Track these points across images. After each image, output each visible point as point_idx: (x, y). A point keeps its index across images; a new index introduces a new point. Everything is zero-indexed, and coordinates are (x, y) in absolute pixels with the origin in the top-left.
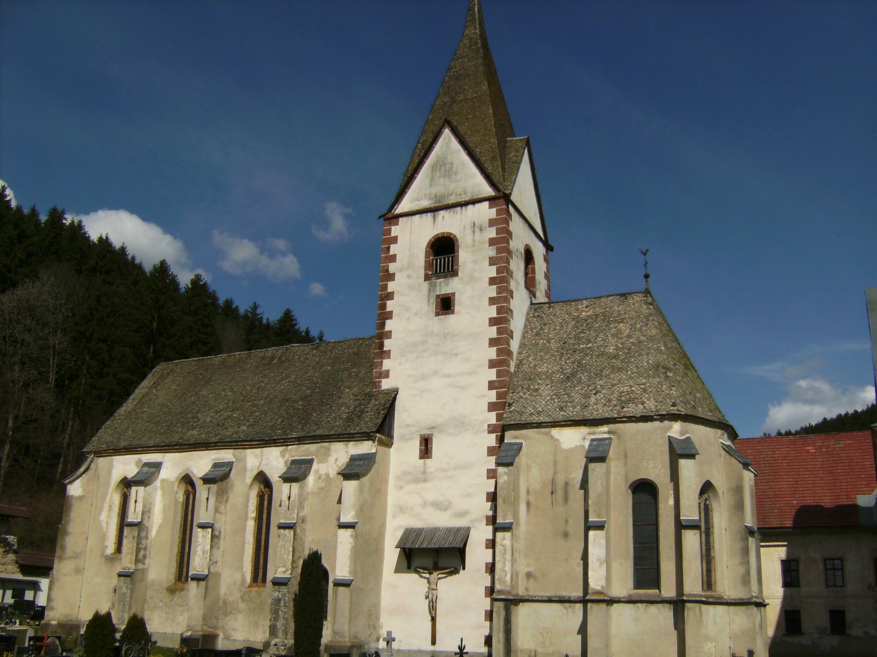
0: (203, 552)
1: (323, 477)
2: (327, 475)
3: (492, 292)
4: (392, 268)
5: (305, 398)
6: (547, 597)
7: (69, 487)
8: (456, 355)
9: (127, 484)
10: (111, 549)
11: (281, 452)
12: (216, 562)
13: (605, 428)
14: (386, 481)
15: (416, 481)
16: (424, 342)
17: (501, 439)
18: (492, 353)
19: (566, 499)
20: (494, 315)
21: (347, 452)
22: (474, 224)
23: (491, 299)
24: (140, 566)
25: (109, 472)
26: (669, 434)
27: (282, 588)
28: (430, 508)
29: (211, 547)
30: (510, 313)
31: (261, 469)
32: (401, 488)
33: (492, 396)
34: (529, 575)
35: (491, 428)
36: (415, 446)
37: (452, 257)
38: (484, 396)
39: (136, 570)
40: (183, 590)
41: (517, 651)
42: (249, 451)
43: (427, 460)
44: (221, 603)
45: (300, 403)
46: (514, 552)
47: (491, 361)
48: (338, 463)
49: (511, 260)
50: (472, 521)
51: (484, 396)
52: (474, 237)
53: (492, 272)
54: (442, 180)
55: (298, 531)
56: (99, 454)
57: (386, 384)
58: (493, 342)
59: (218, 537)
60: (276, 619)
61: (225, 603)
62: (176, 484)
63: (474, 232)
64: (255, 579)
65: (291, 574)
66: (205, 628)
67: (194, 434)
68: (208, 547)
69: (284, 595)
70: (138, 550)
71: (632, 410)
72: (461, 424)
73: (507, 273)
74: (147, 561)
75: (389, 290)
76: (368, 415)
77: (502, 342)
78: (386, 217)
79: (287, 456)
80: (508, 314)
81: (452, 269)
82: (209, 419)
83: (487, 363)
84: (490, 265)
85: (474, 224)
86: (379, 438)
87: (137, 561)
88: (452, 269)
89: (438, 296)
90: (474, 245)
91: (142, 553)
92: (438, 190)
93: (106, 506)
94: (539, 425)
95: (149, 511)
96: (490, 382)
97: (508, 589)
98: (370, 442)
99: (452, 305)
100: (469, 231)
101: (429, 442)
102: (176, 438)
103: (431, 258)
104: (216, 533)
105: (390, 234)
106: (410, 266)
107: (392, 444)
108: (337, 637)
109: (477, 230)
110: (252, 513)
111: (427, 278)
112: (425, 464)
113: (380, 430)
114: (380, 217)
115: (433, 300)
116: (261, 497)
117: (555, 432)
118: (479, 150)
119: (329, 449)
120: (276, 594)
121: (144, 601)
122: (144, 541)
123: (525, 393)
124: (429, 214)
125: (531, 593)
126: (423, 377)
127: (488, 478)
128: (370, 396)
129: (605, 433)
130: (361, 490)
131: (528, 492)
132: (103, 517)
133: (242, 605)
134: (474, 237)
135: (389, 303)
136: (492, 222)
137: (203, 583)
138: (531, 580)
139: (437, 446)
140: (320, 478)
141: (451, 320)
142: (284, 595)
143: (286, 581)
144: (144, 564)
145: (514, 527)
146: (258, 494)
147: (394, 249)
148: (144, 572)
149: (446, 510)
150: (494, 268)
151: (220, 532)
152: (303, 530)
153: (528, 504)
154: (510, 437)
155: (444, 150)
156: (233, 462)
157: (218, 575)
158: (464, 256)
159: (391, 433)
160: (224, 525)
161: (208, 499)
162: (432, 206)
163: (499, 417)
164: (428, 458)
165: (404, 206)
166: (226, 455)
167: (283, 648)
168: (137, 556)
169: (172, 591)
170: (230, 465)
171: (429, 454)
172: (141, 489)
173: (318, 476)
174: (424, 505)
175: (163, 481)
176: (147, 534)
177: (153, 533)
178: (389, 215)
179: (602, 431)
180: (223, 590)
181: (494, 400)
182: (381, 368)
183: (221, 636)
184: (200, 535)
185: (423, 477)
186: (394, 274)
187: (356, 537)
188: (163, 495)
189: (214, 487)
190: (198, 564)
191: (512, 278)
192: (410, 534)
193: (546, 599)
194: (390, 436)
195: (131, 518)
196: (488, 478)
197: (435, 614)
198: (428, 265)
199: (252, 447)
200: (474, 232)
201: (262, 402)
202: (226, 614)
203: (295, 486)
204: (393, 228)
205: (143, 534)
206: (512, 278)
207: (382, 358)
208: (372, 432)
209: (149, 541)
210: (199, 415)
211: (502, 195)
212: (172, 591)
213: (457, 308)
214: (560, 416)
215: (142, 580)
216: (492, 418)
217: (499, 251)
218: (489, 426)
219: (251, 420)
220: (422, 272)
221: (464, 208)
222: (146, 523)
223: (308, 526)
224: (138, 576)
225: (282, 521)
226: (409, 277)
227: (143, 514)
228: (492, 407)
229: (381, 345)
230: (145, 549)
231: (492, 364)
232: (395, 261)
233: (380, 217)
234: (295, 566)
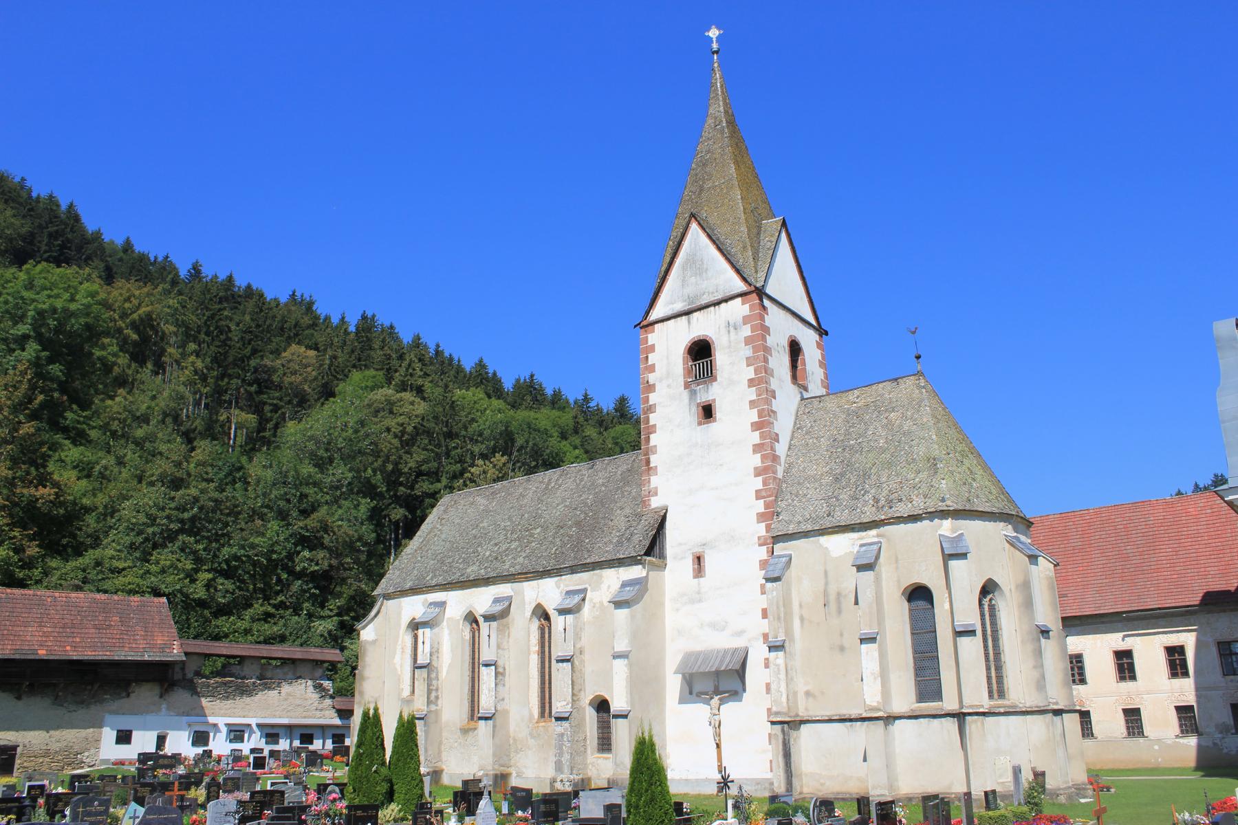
1: (597, 605)
2: (601, 603)
3: (752, 394)
4: (652, 378)
5: (578, 524)
6: (828, 716)
7: (362, 632)
8: (721, 465)
9: (415, 626)
10: (406, 692)
11: (556, 583)
12: (503, 699)
13: (874, 532)
14: (663, 604)
15: (692, 601)
18: (757, 460)
19: (839, 611)
20: (756, 419)
21: (618, 578)
22: (729, 323)
24: (433, 707)
25: (399, 614)
27: (564, 722)
29: (496, 685)
30: (772, 414)
31: (538, 601)
32: (677, 610)
33: (760, 506)
34: (808, 694)
35: (762, 541)
36: (689, 565)
37: (711, 361)
39: (430, 712)
40: (475, 729)
41: (801, 775)
42: (526, 584)
43: (701, 579)
44: (511, 742)
45: (574, 529)
46: (790, 672)
47: (756, 469)
48: (610, 590)
49: (769, 357)
50: (749, 641)
52: (729, 337)
53: (750, 373)
54: (693, 280)
55: (576, 662)
56: (387, 597)
57: (655, 503)
58: (757, 448)
59: (503, 674)
60: (561, 754)
61: (515, 740)
62: (461, 622)
63: (729, 332)
64: (542, 714)
65: (572, 707)
66: (496, 767)
67: (472, 571)
68: (493, 685)
69: (566, 730)
70: (429, 692)
71: (903, 509)
73: (766, 372)
74: (439, 702)
75: (651, 403)
76: (636, 539)
78: (641, 325)
79: (562, 585)
80: (770, 416)
81: (711, 373)
82: (488, 553)
83: (752, 471)
84: (748, 365)
85: (729, 323)
86: (649, 561)
87: (429, 702)
88: (711, 373)
89: (698, 405)
90: (729, 347)
91: (433, 695)
92: (690, 290)
93: (399, 647)
94: (806, 534)
95: (438, 651)
97: (785, 710)
98: (640, 567)
99: (713, 412)
100: (723, 331)
101: (702, 560)
102: (454, 578)
103: (690, 364)
104: (500, 670)
105: (647, 343)
107: (666, 565)
108: (618, 769)
109: (732, 329)
110: (535, 648)
111: (687, 386)
112: (699, 584)
113: (648, 553)
114: (635, 326)
115: (694, 409)
116: (542, 629)
117: (824, 540)
118: (729, 242)
119: (601, 576)
121: (440, 743)
122: (434, 682)
123: (793, 500)
124: (684, 317)
125: (811, 713)
128: (639, 516)
129: (873, 536)
130: (633, 617)
131: (801, 606)
132: (397, 659)
133: (531, 742)
134: (729, 337)
135: (651, 416)
136: (746, 320)
137: (490, 722)
138: (811, 699)
140: (594, 607)
141: (713, 427)
142: (566, 730)
143: (567, 715)
144: (437, 705)
145: (787, 645)
146: (539, 627)
147: (652, 358)
148: (437, 713)
149: (723, 630)
150: (752, 369)
151: (504, 669)
152: (582, 662)
153: (802, 619)
154: (780, 549)
155: (693, 246)
156: (512, 597)
157: (506, 712)
158: (721, 358)
159: (663, 553)
160: (509, 661)
161: (489, 636)
162: (686, 308)
163: (768, 528)
164: (701, 577)
166: (504, 589)
167: (568, 783)
168: (428, 698)
169: (465, 731)
170: (510, 599)
171: (703, 573)
172: (427, 631)
173: (592, 605)
175: (449, 619)
176: (437, 675)
177: (443, 673)
178: (645, 323)
179: (871, 535)
180: (512, 727)
181: (762, 510)
183: (514, 774)
184: (485, 673)
185: (697, 598)
186: (654, 385)
187: (630, 666)
188: (449, 634)
189: (494, 624)
190: (486, 702)
191: (773, 377)
192: (689, 658)
193: (827, 718)
194: (662, 556)
195: (421, 660)
197: (719, 740)
198: (688, 372)
199: (528, 580)
200: (729, 332)
201: (538, 530)
202: (517, 752)
203: (570, 618)
204: (650, 336)
205: (433, 675)
206: (773, 377)
207: (649, 475)
208: (639, 555)
210: (479, 549)
211: (753, 289)
212: (465, 731)
214: (828, 523)
215: (436, 722)
217: (755, 350)
218: (759, 538)
219: (528, 551)
220: (681, 381)
221: (717, 307)
222: (434, 663)
223: (586, 657)
224: (432, 718)
225: (560, 654)
226: (669, 386)
227: (431, 655)
229: (648, 462)
230: (437, 690)
231: (758, 472)
232: (654, 371)
233: (635, 326)
234: (575, 699)
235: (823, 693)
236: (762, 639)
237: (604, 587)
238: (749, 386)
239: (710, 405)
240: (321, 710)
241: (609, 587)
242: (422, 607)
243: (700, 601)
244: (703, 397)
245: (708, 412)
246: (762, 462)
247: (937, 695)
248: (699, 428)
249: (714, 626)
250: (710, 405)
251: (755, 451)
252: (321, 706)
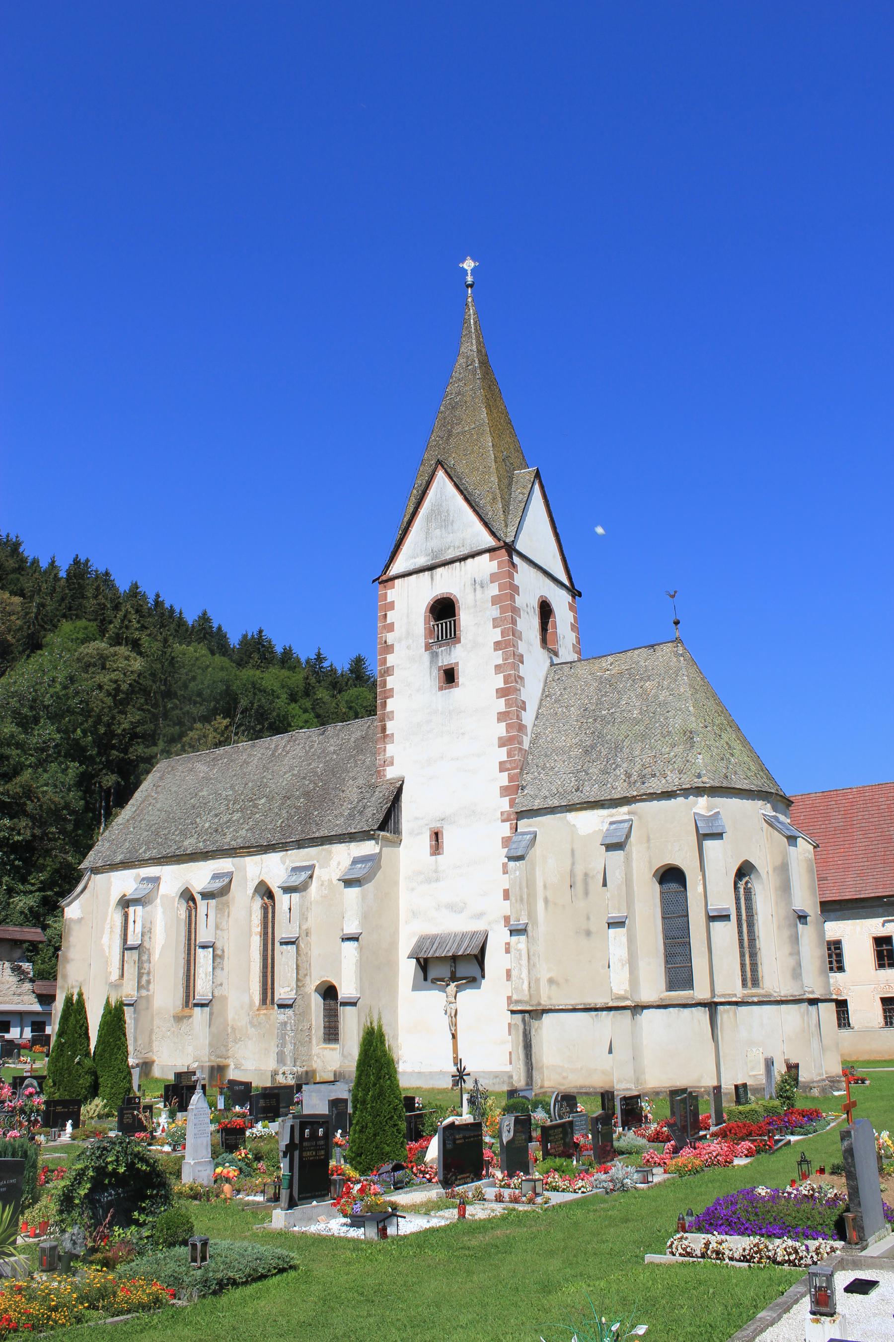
1: (326, 883)
2: (330, 881)
3: (498, 658)
4: (390, 638)
5: (306, 794)
6: (572, 1005)
7: (66, 909)
8: (463, 734)
9: (125, 903)
10: (115, 976)
12: (221, 985)
13: (625, 809)
14: (396, 883)
15: (429, 881)
18: (501, 730)
19: (586, 893)
20: (502, 685)
21: (349, 854)
22: (475, 581)
24: (144, 993)
25: (109, 890)
27: (287, 1010)
30: (519, 680)
31: (262, 878)
32: (413, 889)
33: (504, 779)
34: (551, 981)
36: (426, 841)
37: (455, 621)
39: (140, 997)
40: (190, 1016)
41: (542, 1068)
42: (248, 859)
44: (230, 1030)
45: (302, 800)
46: (532, 957)
47: (500, 739)
48: (340, 867)
49: (518, 619)
50: (489, 923)
52: (475, 596)
53: (496, 635)
54: (438, 532)
55: (302, 945)
56: (96, 871)
57: (391, 773)
58: (502, 717)
59: (222, 957)
60: (283, 1045)
61: (233, 1029)
62: (177, 899)
63: (475, 590)
64: (264, 1001)
65: (296, 994)
66: (213, 1058)
67: (190, 844)
68: (211, 969)
69: (289, 1018)
71: (656, 785)
73: (513, 635)
74: (151, 987)
75: (388, 665)
76: (369, 812)
78: (380, 580)
79: (288, 861)
80: (517, 682)
81: (455, 634)
82: (207, 825)
83: (496, 742)
84: (494, 627)
85: (475, 581)
86: (383, 836)
87: (140, 987)
88: (455, 634)
89: (440, 668)
90: (475, 606)
91: (145, 978)
92: (434, 544)
93: (107, 927)
94: (552, 810)
96: (501, 763)
97: (526, 998)
98: (373, 842)
99: (456, 677)
100: (469, 589)
102: (172, 850)
103: (432, 623)
104: (219, 952)
105: (386, 599)
107: (401, 841)
108: (346, 1061)
109: (478, 587)
110: (257, 929)
111: (428, 647)
113: (383, 827)
114: (374, 581)
115: (435, 672)
116: (265, 909)
117: (572, 817)
118: (478, 492)
119: (330, 852)
121: (151, 1032)
122: (146, 965)
123: (539, 773)
124: (426, 573)
125: (554, 1002)
128: (373, 787)
129: (625, 814)
130: (364, 897)
131: (545, 887)
132: (105, 940)
133: (251, 1031)
134: (475, 596)
135: (389, 679)
136: (493, 578)
137: (207, 1009)
138: (554, 987)
139: (447, 839)
140: (322, 885)
141: (455, 692)
142: (289, 1018)
143: (290, 1002)
144: (148, 990)
145: (529, 929)
146: (262, 906)
147: (391, 616)
148: (148, 999)
149: (461, 912)
151: (223, 951)
152: (308, 944)
153: (546, 901)
154: (525, 825)
155: (439, 496)
156: (232, 873)
157: (224, 998)
158: (465, 617)
159: (398, 828)
160: (229, 943)
161: (207, 915)
162: (429, 563)
163: (512, 803)
164: (439, 854)
166: (224, 865)
167: (291, 1076)
168: (139, 982)
169: (179, 1019)
170: (230, 875)
171: (440, 850)
172: (139, 909)
173: (320, 883)
175: (163, 895)
176: (149, 957)
177: (156, 955)
178: (384, 578)
179: (622, 812)
180: (231, 1015)
181: (506, 783)
182: (384, 755)
183: (232, 1066)
185: (435, 877)
187: (361, 949)
188: (164, 912)
189: (213, 902)
190: (203, 988)
191: (521, 640)
192: (423, 941)
193: (571, 1007)
194: (397, 831)
195: (132, 941)
197: (456, 1030)
198: (430, 632)
199: (250, 854)
200: (475, 590)
201: (263, 801)
202: (236, 1041)
203: (295, 896)
204: (389, 592)
205: (145, 958)
206: (521, 640)
207: (385, 743)
208: (372, 830)
209: (151, 965)
210: (198, 820)
211: (503, 544)
212: (179, 1019)
214: (576, 798)
215: (147, 1008)
217: (503, 610)
219: (251, 823)
220: (422, 642)
221: (463, 562)
222: (146, 944)
223: (313, 939)
224: (142, 1005)
225: (283, 936)
226: (408, 647)
227: (142, 936)
229: (384, 729)
230: (149, 973)
231: (503, 742)
232: (392, 630)
233: (374, 581)
234: (300, 984)
236: (503, 922)
237: (333, 863)
238: (495, 650)
239: (453, 669)
240: (19, 995)
241: (339, 864)
242: (134, 883)
243: (437, 880)
244: (445, 660)
245: (450, 676)
246: (507, 731)
247: (687, 982)
249: (452, 907)
250: (453, 669)
252: (19, 991)
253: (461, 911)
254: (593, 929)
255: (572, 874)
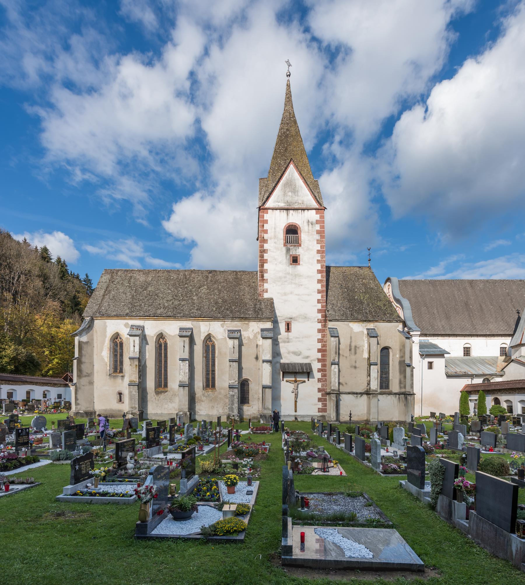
0: (184, 373)
8: (301, 285)
16: (285, 277)
17: (325, 326)
23: (318, 260)
26: (398, 329)
28: (291, 354)
35: (319, 321)
38: (315, 306)
43: (289, 333)
47: (318, 290)
50: (311, 361)
51: (315, 306)
72: (305, 318)
77: (323, 282)
84: (317, 243)
90: (309, 232)
101: (290, 325)
106: (275, 237)
112: (288, 335)
120: (231, 393)
126: (285, 294)
127: (318, 342)
139: (293, 326)
141: (299, 267)
150: (319, 245)
158: (304, 236)
164: (289, 332)
165: (268, 205)
174: (289, 353)
196: (318, 342)
213: (301, 263)
216: (319, 316)
218: (318, 320)
228: (319, 311)
235: (346, 384)
236: (317, 361)
237: (250, 330)
238: (317, 253)
239: (297, 257)
241: (253, 330)
243: (288, 342)
244: (293, 252)
245: (295, 260)
246: (322, 288)
248: (291, 266)
249: (295, 353)
250: (297, 257)
251: (318, 282)
253: (299, 355)
254: (357, 366)
255: (350, 346)
